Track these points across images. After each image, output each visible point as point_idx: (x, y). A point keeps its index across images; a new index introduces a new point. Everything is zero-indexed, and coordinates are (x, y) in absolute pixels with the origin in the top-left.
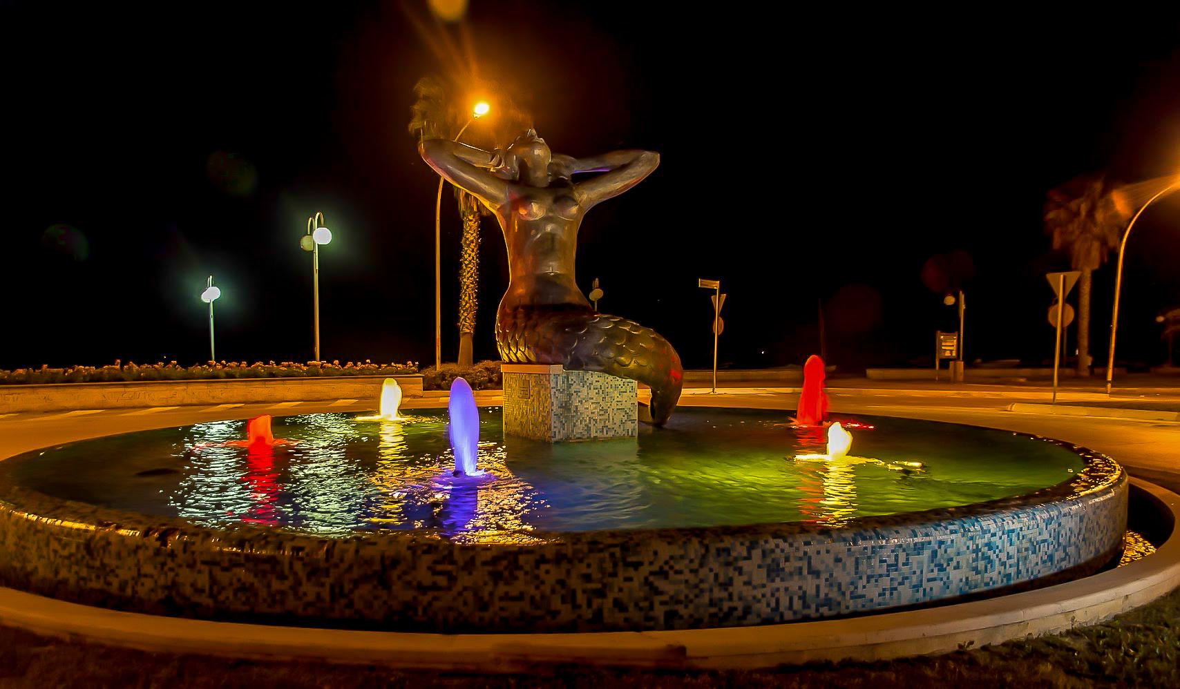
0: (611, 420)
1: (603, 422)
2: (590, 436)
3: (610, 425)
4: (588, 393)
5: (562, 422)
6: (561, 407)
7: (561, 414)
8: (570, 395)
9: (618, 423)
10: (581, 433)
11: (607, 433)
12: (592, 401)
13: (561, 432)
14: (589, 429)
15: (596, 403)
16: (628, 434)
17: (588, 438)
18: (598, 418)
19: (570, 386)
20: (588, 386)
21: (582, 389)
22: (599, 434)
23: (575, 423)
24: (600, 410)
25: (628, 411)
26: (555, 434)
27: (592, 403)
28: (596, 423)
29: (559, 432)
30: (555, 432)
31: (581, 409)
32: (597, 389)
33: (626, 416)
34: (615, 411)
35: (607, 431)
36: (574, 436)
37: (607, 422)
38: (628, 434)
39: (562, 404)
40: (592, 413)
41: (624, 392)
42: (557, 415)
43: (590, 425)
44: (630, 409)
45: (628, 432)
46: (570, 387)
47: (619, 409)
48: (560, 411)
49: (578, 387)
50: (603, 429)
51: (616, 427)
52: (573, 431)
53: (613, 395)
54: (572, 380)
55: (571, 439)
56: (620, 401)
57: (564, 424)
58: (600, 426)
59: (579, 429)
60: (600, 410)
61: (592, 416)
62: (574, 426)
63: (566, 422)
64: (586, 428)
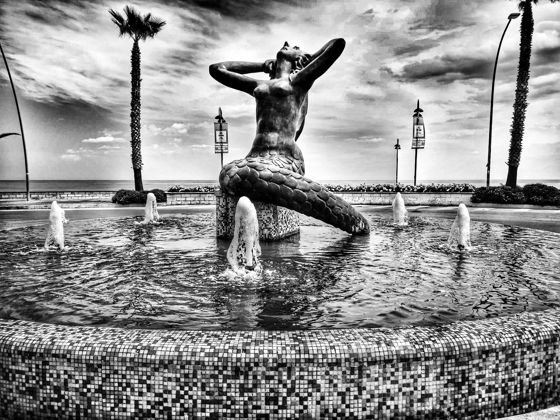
19: (227, 204)
49: (232, 204)
52: (229, 231)
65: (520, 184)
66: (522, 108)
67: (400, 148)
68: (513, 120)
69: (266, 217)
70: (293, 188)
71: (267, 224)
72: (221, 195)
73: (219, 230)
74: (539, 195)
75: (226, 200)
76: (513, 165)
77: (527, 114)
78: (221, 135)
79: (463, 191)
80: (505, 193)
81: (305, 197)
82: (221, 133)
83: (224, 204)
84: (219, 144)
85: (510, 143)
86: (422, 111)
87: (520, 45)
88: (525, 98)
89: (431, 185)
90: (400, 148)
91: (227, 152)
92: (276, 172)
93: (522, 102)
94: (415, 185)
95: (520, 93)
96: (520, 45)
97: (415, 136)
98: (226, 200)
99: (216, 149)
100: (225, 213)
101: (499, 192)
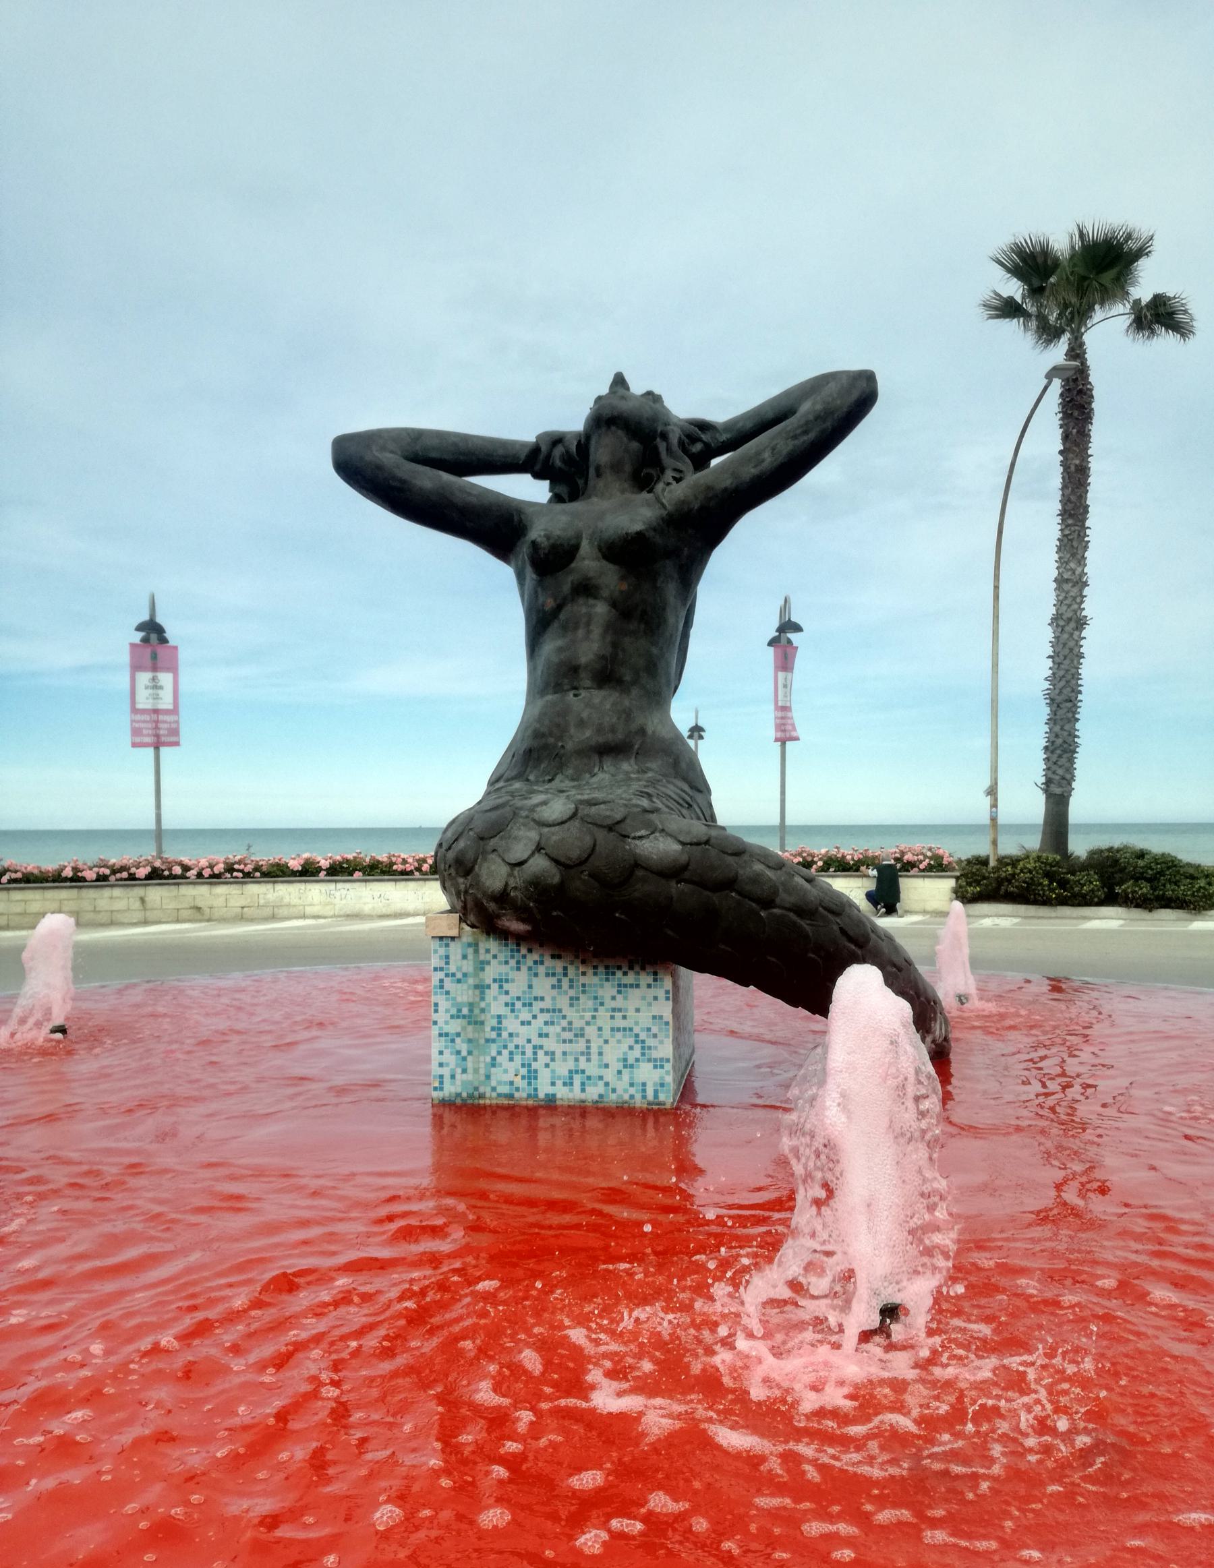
0: (594, 1057)
1: (571, 1059)
2: (536, 1096)
3: (592, 1069)
4: (530, 987)
5: (458, 1052)
6: (458, 1017)
7: (458, 1035)
8: (481, 988)
9: (616, 1065)
10: (512, 1083)
11: (583, 1090)
12: (541, 1005)
13: (458, 1076)
14: (532, 1076)
15: (554, 1011)
16: (644, 1097)
17: (529, 1096)
18: (559, 1049)
19: (481, 966)
20: (530, 969)
21: (513, 974)
22: (563, 1093)
23: (494, 1059)
24: (564, 1029)
25: (643, 1036)
26: (441, 1083)
27: (542, 1011)
28: (553, 1060)
29: (453, 1077)
30: (441, 1077)
31: (511, 1024)
32: (554, 975)
33: (638, 1047)
34: (607, 1033)
35: (583, 1084)
36: (494, 1089)
37: (583, 1059)
38: (644, 1097)
39: (459, 1011)
40: (540, 1035)
41: (631, 986)
42: (447, 1035)
43: (535, 1065)
44: (649, 1029)
45: (644, 1091)
46: (483, 969)
47: (619, 1030)
48: (454, 1026)
49: (504, 969)
50: (571, 1078)
51: (609, 1075)
52: (488, 1077)
53: (600, 993)
54: (488, 951)
55: (482, 1096)
56: (620, 1010)
57: (464, 1059)
58: (562, 1068)
59: (506, 1071)
60: (564, 1029)
61: (544, 1041)
62: (494, 1065)
63: (470, 1053)
64: (524, 1071)
65: (1079, 847)
66: (1077, 628)
67: (701, 737)
68: (1050, 663)
69: (645, 1019)
70: (768, 903)
71: (650, 1042)
72: (455, 933)
73: (446, 1071)
74: (1138, 877)
75: (476, 951)
76: (1058, 791)
77: (1087, 647)
78: (155, 686)
79: (930, 868)
80: (1047, 875)
81: (807, 936)
82: (154, 679)
83: (468, 966)
84: (147, 718)
85: (1046, 728)
86: (797, 628)
87: (1061, 452)
88: (1082, 602)
89: (834, 852)
90: (701, 737)
91: (177, 744)
92: (698, 844)
93: (1075, 612)
94: (783, 849)
95: (1067, 587)
96: (1061, 452)
97: (780, 704)
98: (476, 951)
99: (136, 732)
100: (471, 1006)
101: (1030, 872)
